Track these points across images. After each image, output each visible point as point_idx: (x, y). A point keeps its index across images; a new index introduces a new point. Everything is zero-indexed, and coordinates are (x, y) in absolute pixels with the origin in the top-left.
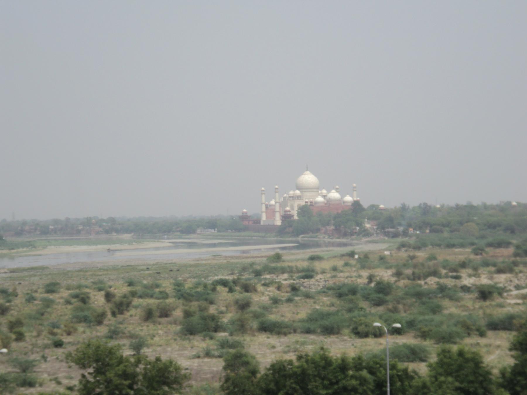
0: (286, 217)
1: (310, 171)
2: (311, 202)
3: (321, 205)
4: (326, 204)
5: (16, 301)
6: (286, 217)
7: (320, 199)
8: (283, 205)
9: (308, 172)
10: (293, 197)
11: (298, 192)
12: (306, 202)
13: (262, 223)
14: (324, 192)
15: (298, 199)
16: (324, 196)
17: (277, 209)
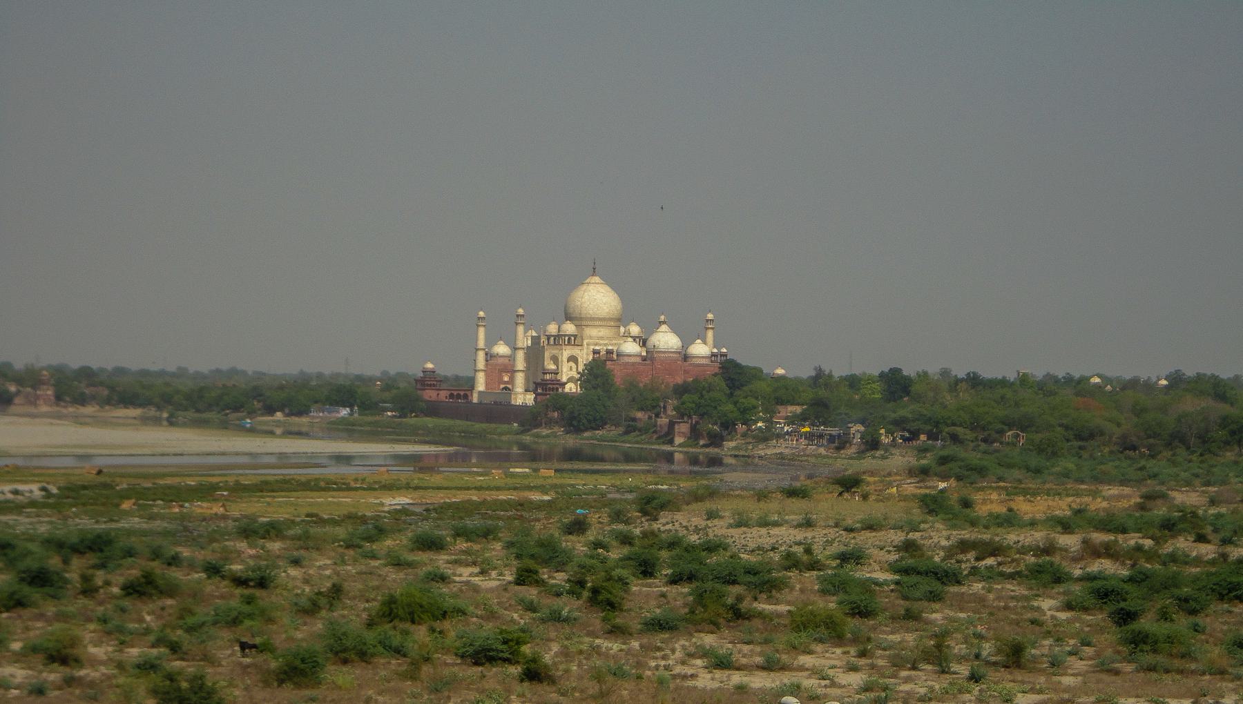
0: (545, 386)
2: (609, 352)
9: (597, 279)
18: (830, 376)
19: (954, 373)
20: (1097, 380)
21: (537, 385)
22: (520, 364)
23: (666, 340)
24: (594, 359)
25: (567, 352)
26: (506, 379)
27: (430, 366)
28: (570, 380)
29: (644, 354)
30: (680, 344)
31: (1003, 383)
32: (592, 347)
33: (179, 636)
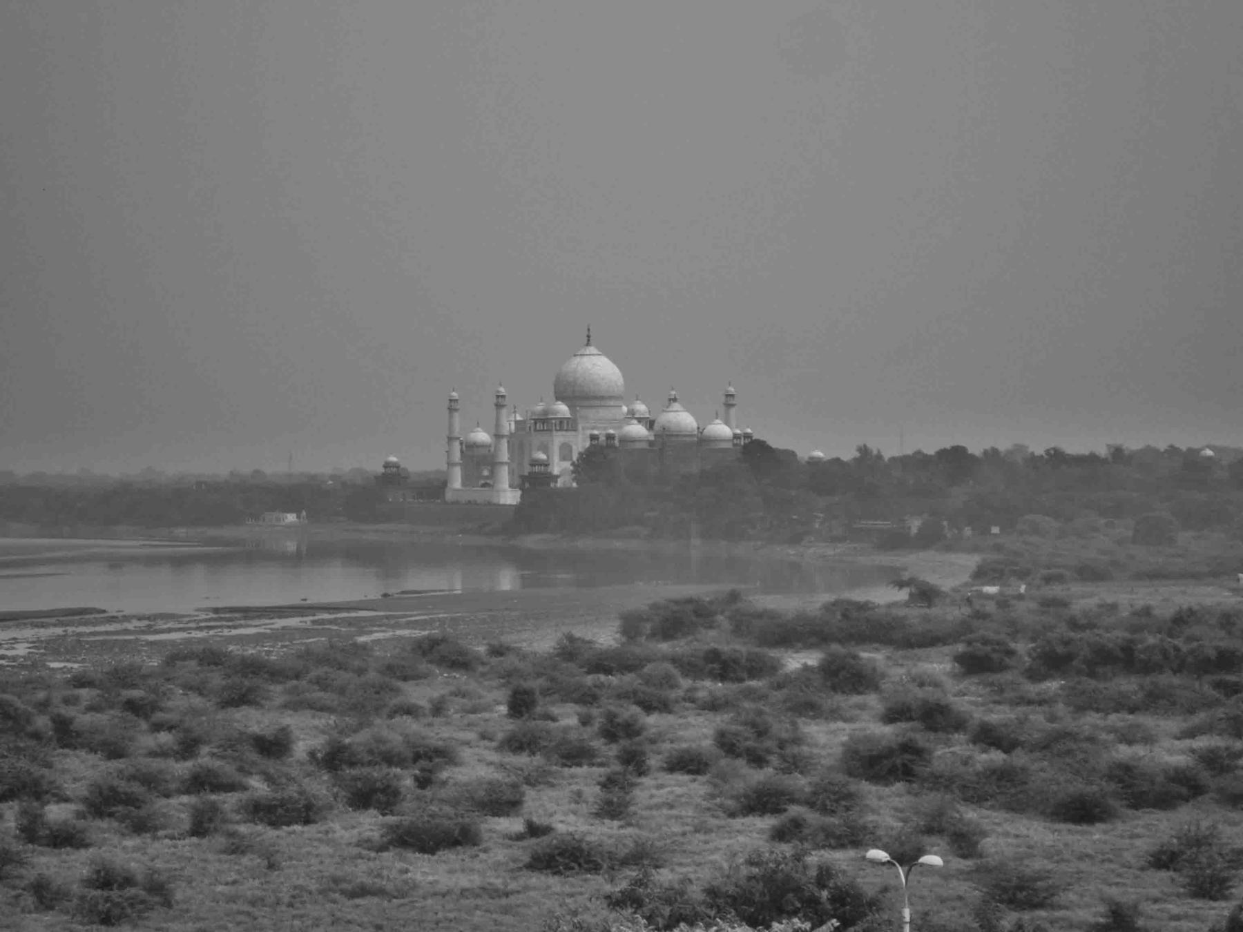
0: (535, 481)
1: (598, 348)
2: (610, 437)
3: (638, 446)
4: (651, 443)
5: (337, 826)
6: (535, 481)
7: (637, 430)
8: (518, 443)
9: (592, 350)
10: (544, 421)
11: (562, 409)
12: (593, 437)
13: (449, 496)
14: (641, 408)
15: (561, 430)
16: (650, 424)
17: (504, 456)
18: (879, 457)
19: (1030, 450)
20: (1209, 453)
21: (524, 478)
22: (504, 456)
23: (683, 419)
24: (591, 445)
25: (558, 439)
26: (486, 473)
27: (393, 459)
28: (563, 472)
29: (652, 438)
30: (695, 425)
31: (1092, 459)
32: (589, 432)
33: (610, 749)
